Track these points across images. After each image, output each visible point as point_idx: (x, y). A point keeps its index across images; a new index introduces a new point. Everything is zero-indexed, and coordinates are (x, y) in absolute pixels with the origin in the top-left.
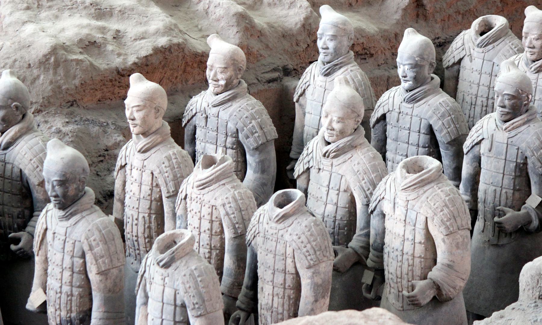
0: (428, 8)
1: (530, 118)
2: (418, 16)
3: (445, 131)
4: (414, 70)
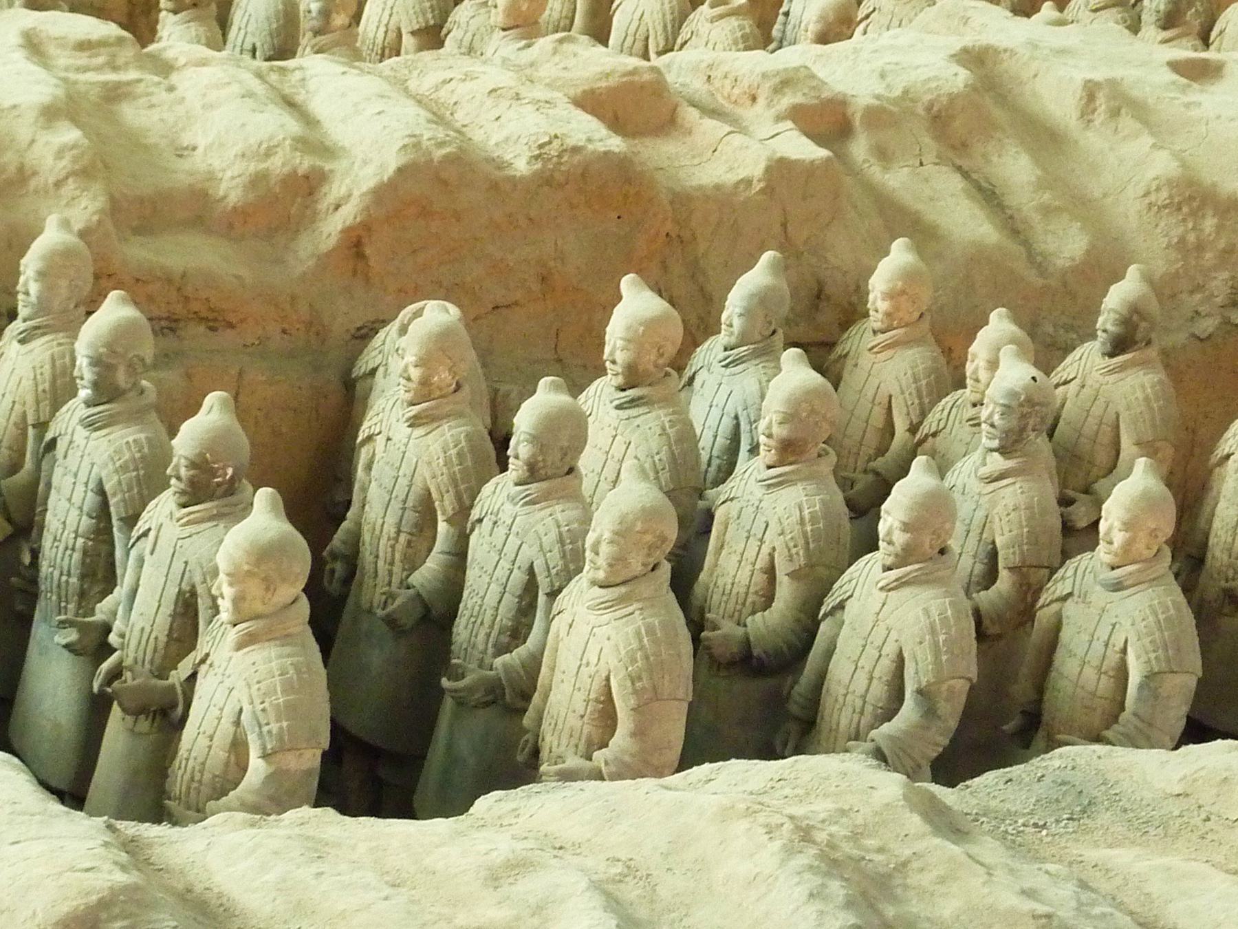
0: (372, 263)
1: (226, 510)
2: (355, 273)
3: (119, 497)
4: (96, 369)
